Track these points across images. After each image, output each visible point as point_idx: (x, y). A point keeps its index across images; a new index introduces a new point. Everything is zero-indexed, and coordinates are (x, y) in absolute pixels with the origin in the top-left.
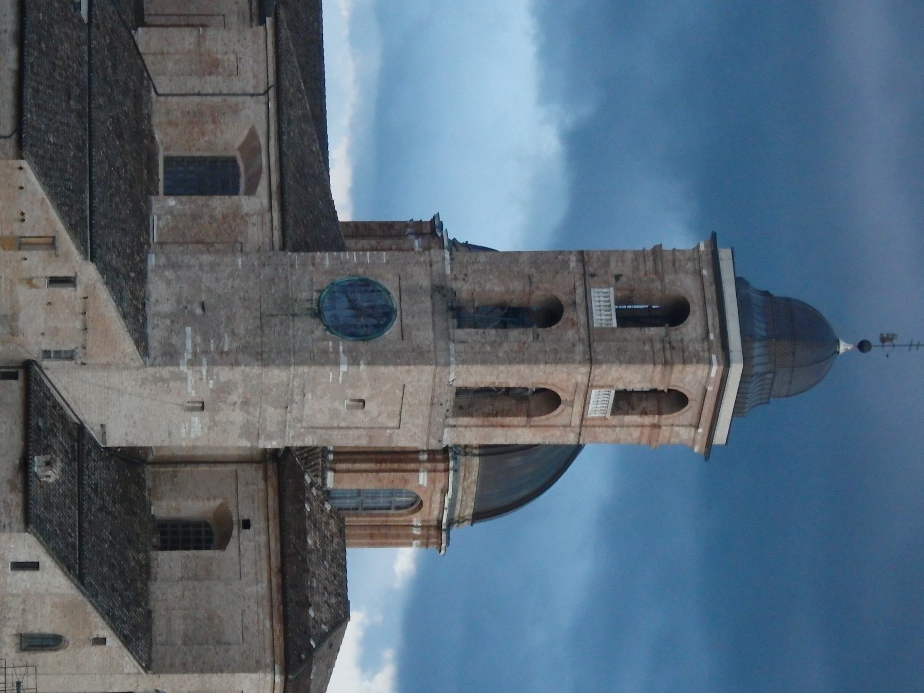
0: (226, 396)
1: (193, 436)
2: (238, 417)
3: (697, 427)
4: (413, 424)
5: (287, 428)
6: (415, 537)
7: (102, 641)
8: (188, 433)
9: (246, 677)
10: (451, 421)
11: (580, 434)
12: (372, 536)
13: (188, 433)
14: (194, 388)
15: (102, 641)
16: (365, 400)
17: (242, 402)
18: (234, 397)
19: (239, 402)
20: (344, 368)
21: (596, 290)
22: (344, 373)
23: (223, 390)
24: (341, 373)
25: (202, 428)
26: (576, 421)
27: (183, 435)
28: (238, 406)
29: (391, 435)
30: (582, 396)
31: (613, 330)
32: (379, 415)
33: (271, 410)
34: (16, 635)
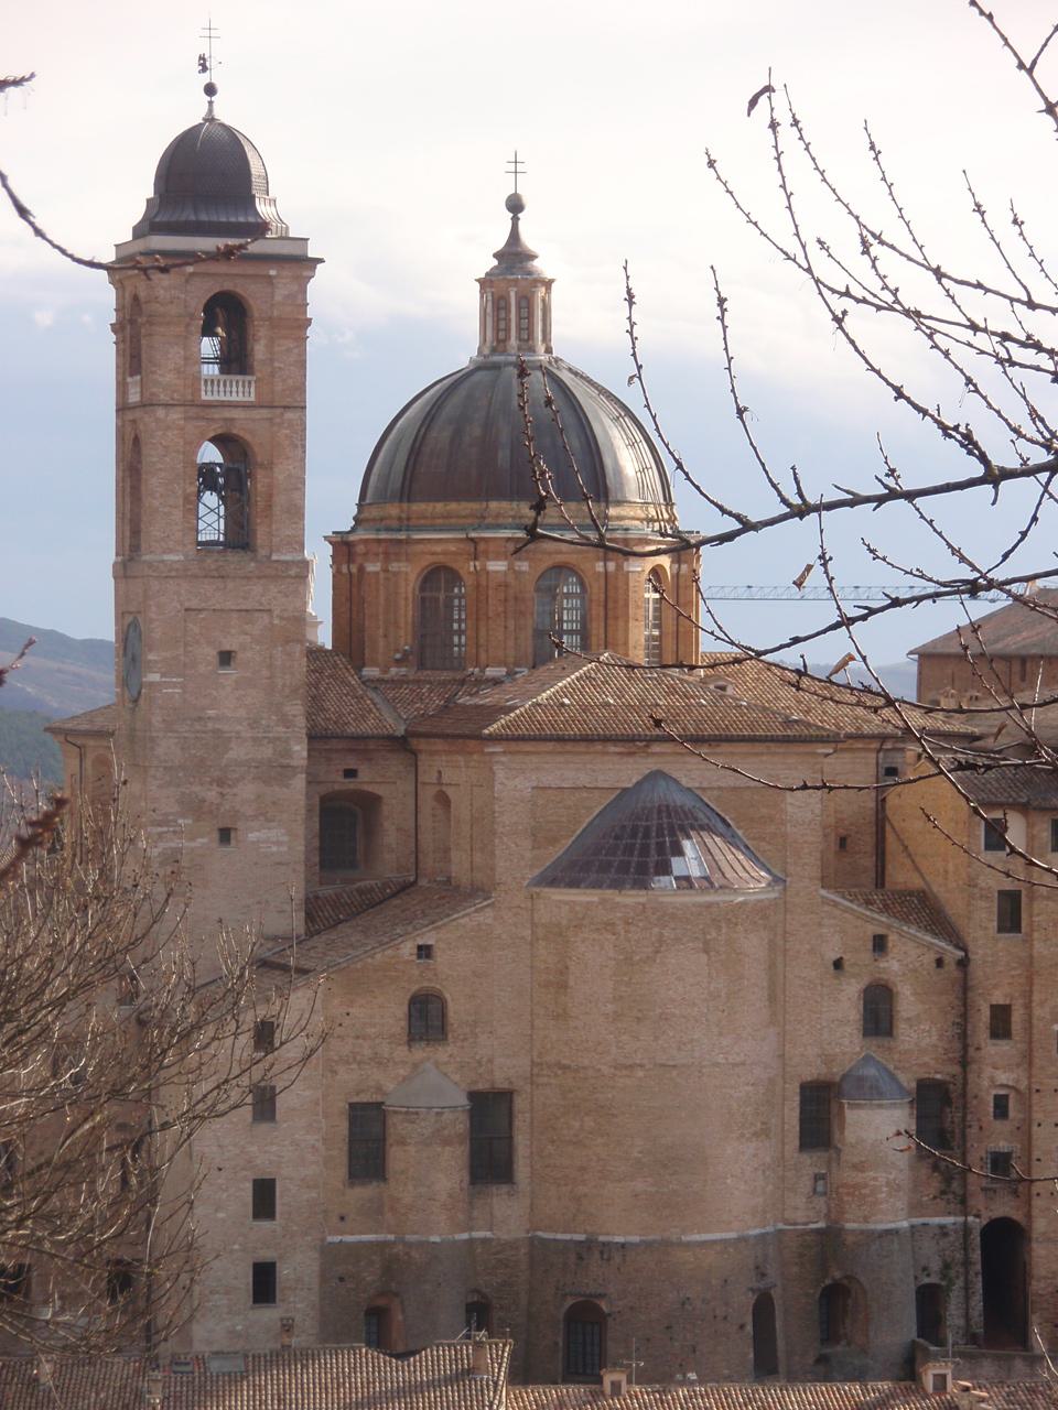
0: (206, 804)
1: (286, 839)
2: (247, 790)
3: (270, 277)
4: (262, 596)
5: (271, 735)
6: (619, 567)
7: (425, 951)
8: (278, 843)
9: (502, 783)
10: (262, 552)
11: (285, 407)
12: (616, 618)
13: (278, 843)
14: (193, 839)
15: (425, 951)
16: (218, 650)
17: (218, 785)
18: (211, 794)
19: (220, 790)
20: (155, 677)
21: (203, 393)
22: (161, 677)
23: (197, 809)
24: (164, 679)
25: (269, 829)
26: (265, 413)
27: (285, 849)
28: (226, 790)
29: (282, 618)
30: (208, 411)
31: (142, 379)
32: (246, 634)
33: (231, 755)
34: (410, 1046)
